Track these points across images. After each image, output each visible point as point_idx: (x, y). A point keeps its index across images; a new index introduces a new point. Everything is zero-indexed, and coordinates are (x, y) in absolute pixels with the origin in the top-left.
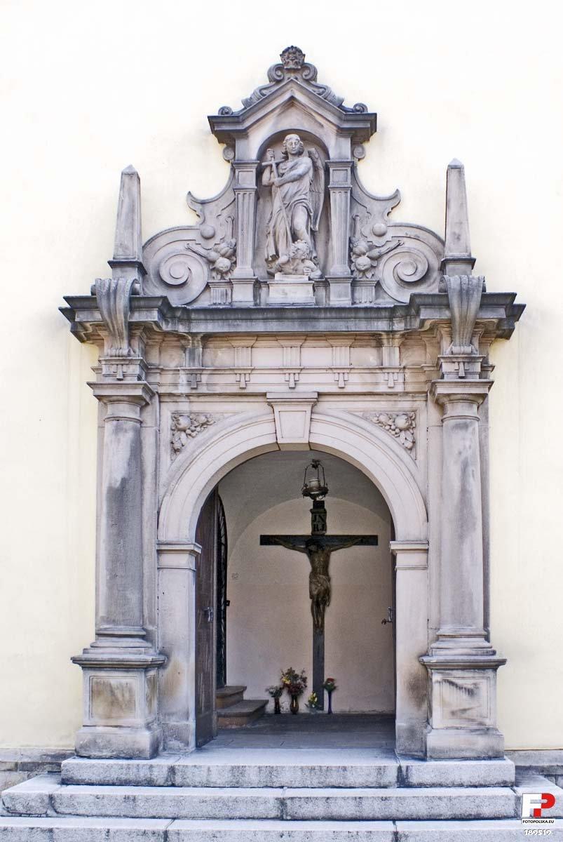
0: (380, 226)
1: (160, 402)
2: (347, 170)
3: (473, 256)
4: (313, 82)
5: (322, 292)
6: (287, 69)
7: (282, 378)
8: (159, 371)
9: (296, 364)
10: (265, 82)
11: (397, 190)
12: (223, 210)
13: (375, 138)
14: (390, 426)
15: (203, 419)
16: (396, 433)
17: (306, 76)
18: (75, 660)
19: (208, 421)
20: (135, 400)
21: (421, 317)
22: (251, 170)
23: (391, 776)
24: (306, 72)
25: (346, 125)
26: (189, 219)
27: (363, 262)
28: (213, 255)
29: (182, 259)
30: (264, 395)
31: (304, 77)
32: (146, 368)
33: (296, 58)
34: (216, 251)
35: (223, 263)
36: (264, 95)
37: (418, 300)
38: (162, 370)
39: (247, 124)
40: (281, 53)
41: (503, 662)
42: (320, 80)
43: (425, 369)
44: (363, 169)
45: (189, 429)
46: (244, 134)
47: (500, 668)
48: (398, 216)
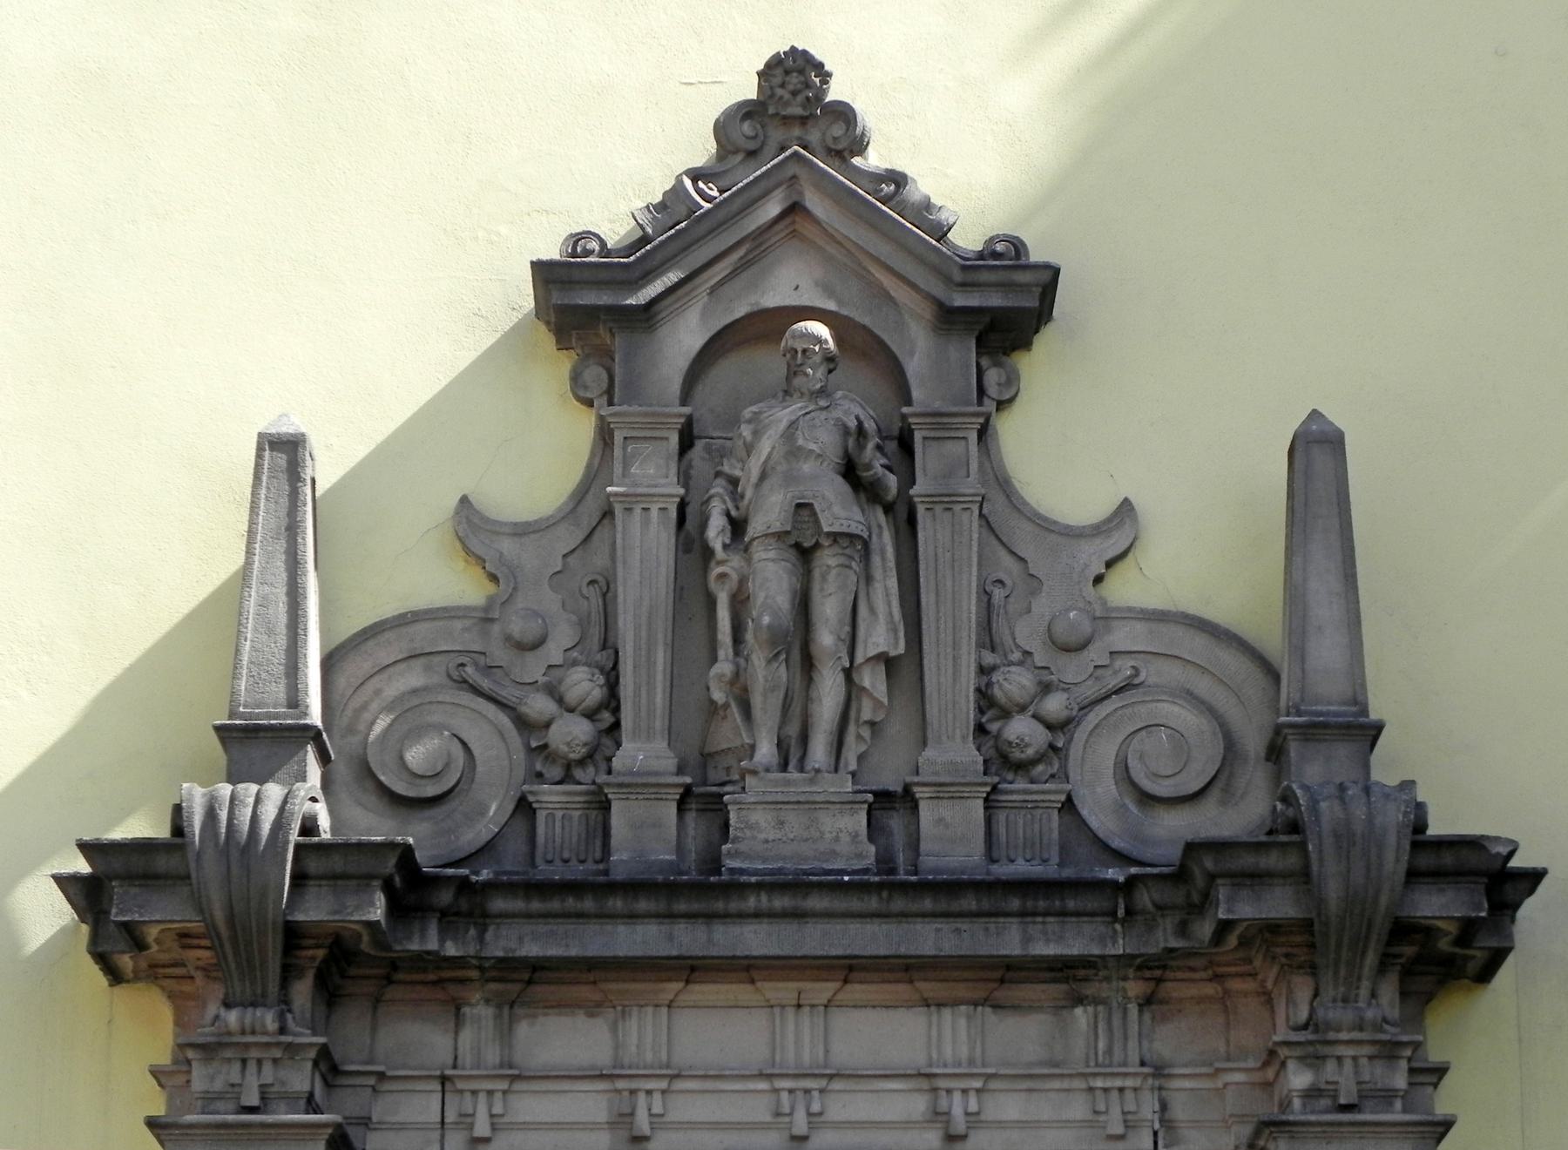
3: (1374, 716)
4: (857, 161)
8: (372, 1081)
11: (1126, 503)
12: (565, 556)
13: (1046, 341)
17: (835, 139)
21: (1222, 915)
22: (664, 434)
24: (838, 130)
25: (960, 300)
27: (1022, 731)
32: (329, 1067)
36: (708, 199)
38: (381, 1076)
44: (1012, 430)
48: (1125, 588)
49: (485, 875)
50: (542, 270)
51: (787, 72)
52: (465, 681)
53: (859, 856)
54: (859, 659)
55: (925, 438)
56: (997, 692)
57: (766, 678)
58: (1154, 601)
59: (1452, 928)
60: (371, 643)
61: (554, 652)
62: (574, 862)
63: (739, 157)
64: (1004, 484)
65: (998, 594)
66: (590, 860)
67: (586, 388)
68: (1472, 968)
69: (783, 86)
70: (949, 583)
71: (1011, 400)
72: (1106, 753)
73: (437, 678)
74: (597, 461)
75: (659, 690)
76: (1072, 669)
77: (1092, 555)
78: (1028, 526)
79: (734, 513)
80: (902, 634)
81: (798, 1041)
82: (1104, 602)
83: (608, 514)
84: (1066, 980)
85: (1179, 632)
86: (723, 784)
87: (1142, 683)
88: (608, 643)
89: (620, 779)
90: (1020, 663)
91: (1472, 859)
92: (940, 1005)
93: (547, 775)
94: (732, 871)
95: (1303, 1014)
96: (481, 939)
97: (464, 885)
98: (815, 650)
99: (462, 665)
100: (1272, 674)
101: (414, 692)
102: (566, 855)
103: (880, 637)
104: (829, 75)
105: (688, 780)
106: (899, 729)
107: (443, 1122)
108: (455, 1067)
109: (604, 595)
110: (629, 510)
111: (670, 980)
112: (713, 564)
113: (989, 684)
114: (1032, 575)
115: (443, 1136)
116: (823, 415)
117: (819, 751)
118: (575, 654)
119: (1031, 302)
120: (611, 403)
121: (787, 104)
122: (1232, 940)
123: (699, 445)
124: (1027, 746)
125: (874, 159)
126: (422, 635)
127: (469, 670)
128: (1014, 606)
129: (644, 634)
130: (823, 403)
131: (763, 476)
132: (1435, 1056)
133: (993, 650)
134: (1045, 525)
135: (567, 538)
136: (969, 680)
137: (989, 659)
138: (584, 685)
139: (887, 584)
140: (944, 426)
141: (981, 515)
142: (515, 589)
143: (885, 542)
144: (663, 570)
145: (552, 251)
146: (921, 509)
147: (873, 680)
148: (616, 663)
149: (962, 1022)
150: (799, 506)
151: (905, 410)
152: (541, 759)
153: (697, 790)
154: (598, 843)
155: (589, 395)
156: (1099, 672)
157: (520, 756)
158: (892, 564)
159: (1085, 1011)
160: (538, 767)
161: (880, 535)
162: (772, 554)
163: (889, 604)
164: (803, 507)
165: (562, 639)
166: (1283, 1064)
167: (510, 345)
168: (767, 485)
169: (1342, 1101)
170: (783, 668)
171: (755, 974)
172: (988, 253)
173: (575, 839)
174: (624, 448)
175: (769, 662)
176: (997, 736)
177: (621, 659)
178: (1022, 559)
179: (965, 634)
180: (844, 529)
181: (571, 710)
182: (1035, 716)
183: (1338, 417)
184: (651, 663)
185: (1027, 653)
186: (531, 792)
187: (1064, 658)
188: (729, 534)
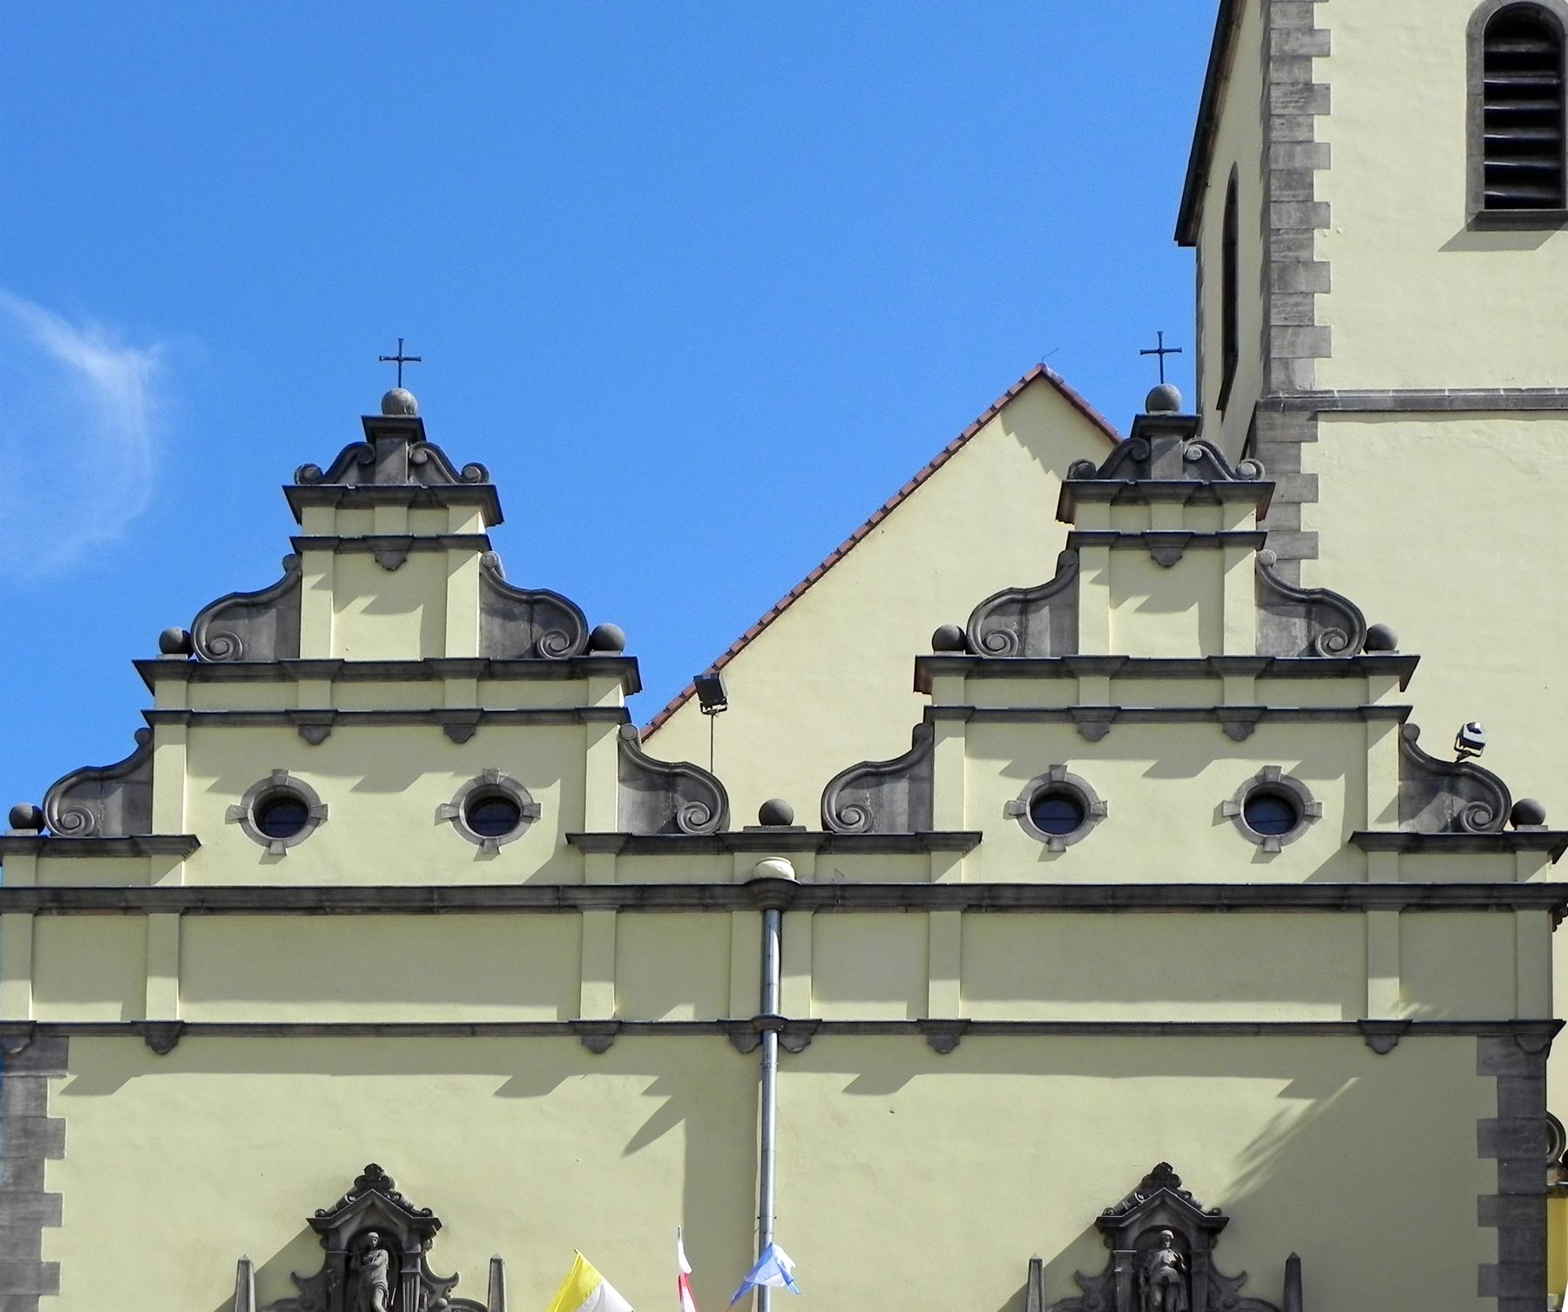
24: (1174, 1182)
58: (1250, 1296)
65: (1211, 1295)
125: (1182, 1188)
134: (1222, 1277)
135: (1102, 1281)
139: (1184, 1292)
167: (1087, 1234)
172: (1211, 1213)
183: (1299, 1253)
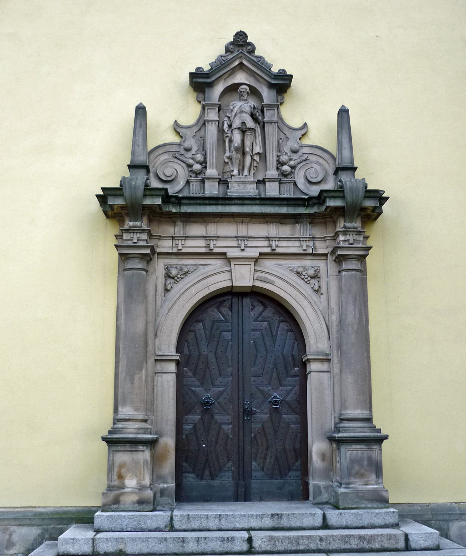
0: (296, 146)
1: (158, 258)
2: (274, 110)
3: (355, 166)
4: (253, 54)
5: (261, 187)
6: (237, 45)
7: (234, 243)
9: (244, 234)
10: (223, 52)
11: (306, 123)
12: (196, 132)
14: (304, 276)
15: (186, 270)
16: (308, 281)
17: (249, 49)
18: (104, 439)
19: (189, 271)
20: (143, 257)
23: (319, 522)
24: (249, 47)
25: (273, 82)
26: (175, 139)
27: (286, 168)
28: (191, 161)
29: (171, 164)
30: (225, 254)
31: (247, 49)
33: (243, 38)
34: (193, 159)
35: (197, 167)
36: (224, 61)
37: (325, 194)
38: (160, 236)
39: (213, 79)
40: (234, 35)
41: (386, 437)
42: (257, 53)
43: (327, 238)
44: (283, 109)
45: (176, 276)
46: (211, 85)
47: (385, 441)
49: (180, 196)
50: (191, 74)
51: (240, 35)
52: (176, 157)
53: (255, 193)
54: (254, 153)
55: (266, 110)
56: (281, 160)
57: (236, 157)
58: (311, 143)
59: (371, 208)
60: (157, 150)
61: (193, 151)
62: (198, 193)
63: (230, 53)
64: (281, 119)
65: (281, 141)
66: (201, 193)
67: (200, 99)
68: (373, 217)
69: (239, 38)
70: (271, 138)
71: (283, 103)
72: (302, 173)
73: (171, 157)
74: (202, 114)
75: (214, 159)
76: (295, 156)
77: (300, 133)
78: (286, 128)
79: (229, 124)
80: (262, 149)
81: (242, 231)
82: (301, 143)
83: (204, 124)
84: (295, 218)
85: (316, 149)
86: (227, 178)
87: (309, 160)
88: (204, 150)
89: (207, 177)
90: (285, 155)
91: (376, 195)
92: (270, 223)
93: (192, 176)
94: (229, 195)
95: (342, 226)
96: (180, 208)
97: (177, 197)
98: (245, 151)
99: (175, 154)
100: (334, 159)
101: (166, 159)
102: (196, 192)
103: (258, 149)
104: (248, 36)
105: (220, 177)
106: (261, 167)
107: (172, 246)
108: (175, 235)
109: (203, 140)
110: (209, 123)
111: (217, 217)
112: (225, 134)
113: (279, 159)
114: (287, 138)
115: (172, 249)
116: (247, 104)
117: (246, 172)
118: (198, 152)
119: (287, 82)
120: (204, 102)
121: (239, 42)
122: (328, 210)
123: (222, 111)
124: (287, 171)
126: (167, 148)
127: (177, 155)
128: (283, 144)
129: (211, 148)
130: (247, 102)
131: (235, 116)
132: (367, 234)
133: (280, 152)
134: (290, 128)
135: (196, 129)
136: (275, 158)
137: (279, 154)
138: (199, 157)
139: (259, 139)
140: (270, 107)
141: (278, 126)
142: (186, 139)
143: (258, 130)
144: (215, 135)
145: (193, 71)
146: (266, 124)
147: (256, 158)
148: (206, 155)
149: (275, 226)
150: (242, 122)
151: (263, 104)
152: (191, 173)
153: (222, 179)
154: (203, 190)
155: (200, 100)
156: (300, 157)
157: (187, 172)
158: (260, 135)
159: (299, 225)
160: (191, 174)
161: (258, 129)
162: (237, 132)
163: (259, 143)
164: (243, 123)
165: (195, 149)
166: (339, 235)
168: (236, 118)
169: (350, 243)
170: (239, 155)
171: (234, 216)
173: (198, 189)
174: (207, 111)
175: (237, 154)
176: (281, 170)
177: (207, 153)
178: (285, 134)
179: (275, 149)
180: (251, 127)
181: (197, 163)
182: (288, 166)
183: (348, 106)
184: (213, 154)
185: (287, 153)
186: (190, 180)
187: (293, 154)
188: (228, 128)
